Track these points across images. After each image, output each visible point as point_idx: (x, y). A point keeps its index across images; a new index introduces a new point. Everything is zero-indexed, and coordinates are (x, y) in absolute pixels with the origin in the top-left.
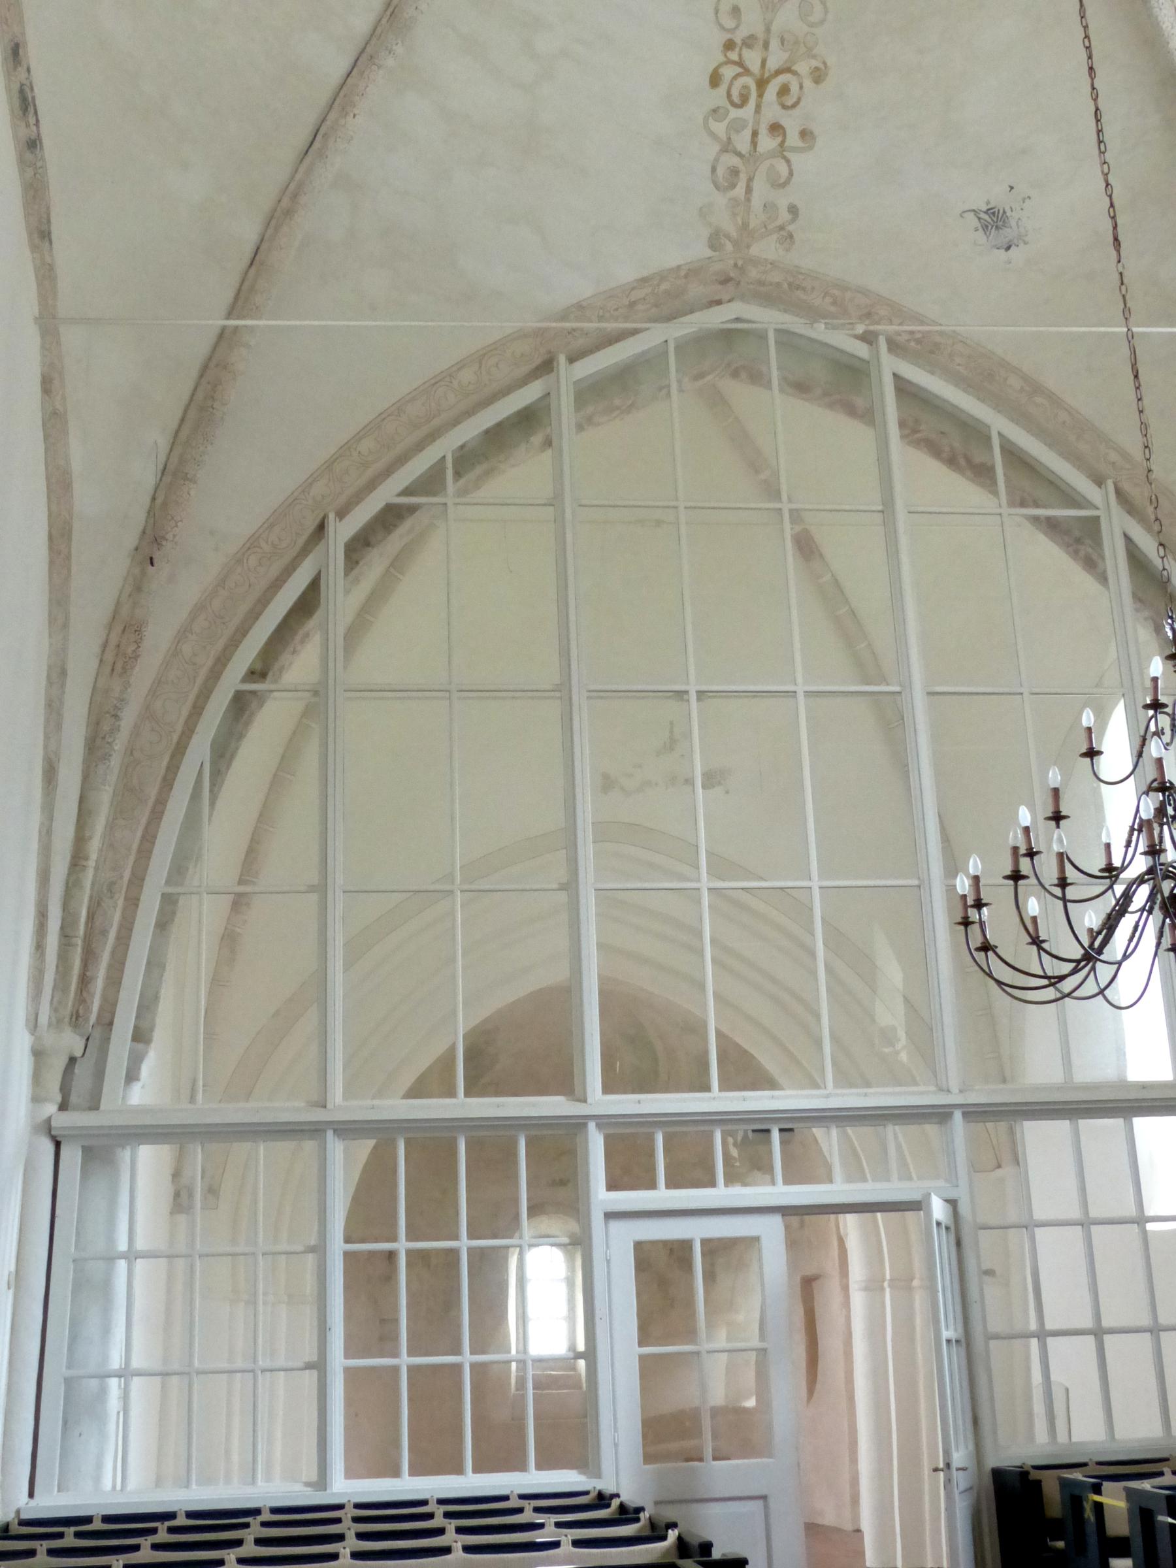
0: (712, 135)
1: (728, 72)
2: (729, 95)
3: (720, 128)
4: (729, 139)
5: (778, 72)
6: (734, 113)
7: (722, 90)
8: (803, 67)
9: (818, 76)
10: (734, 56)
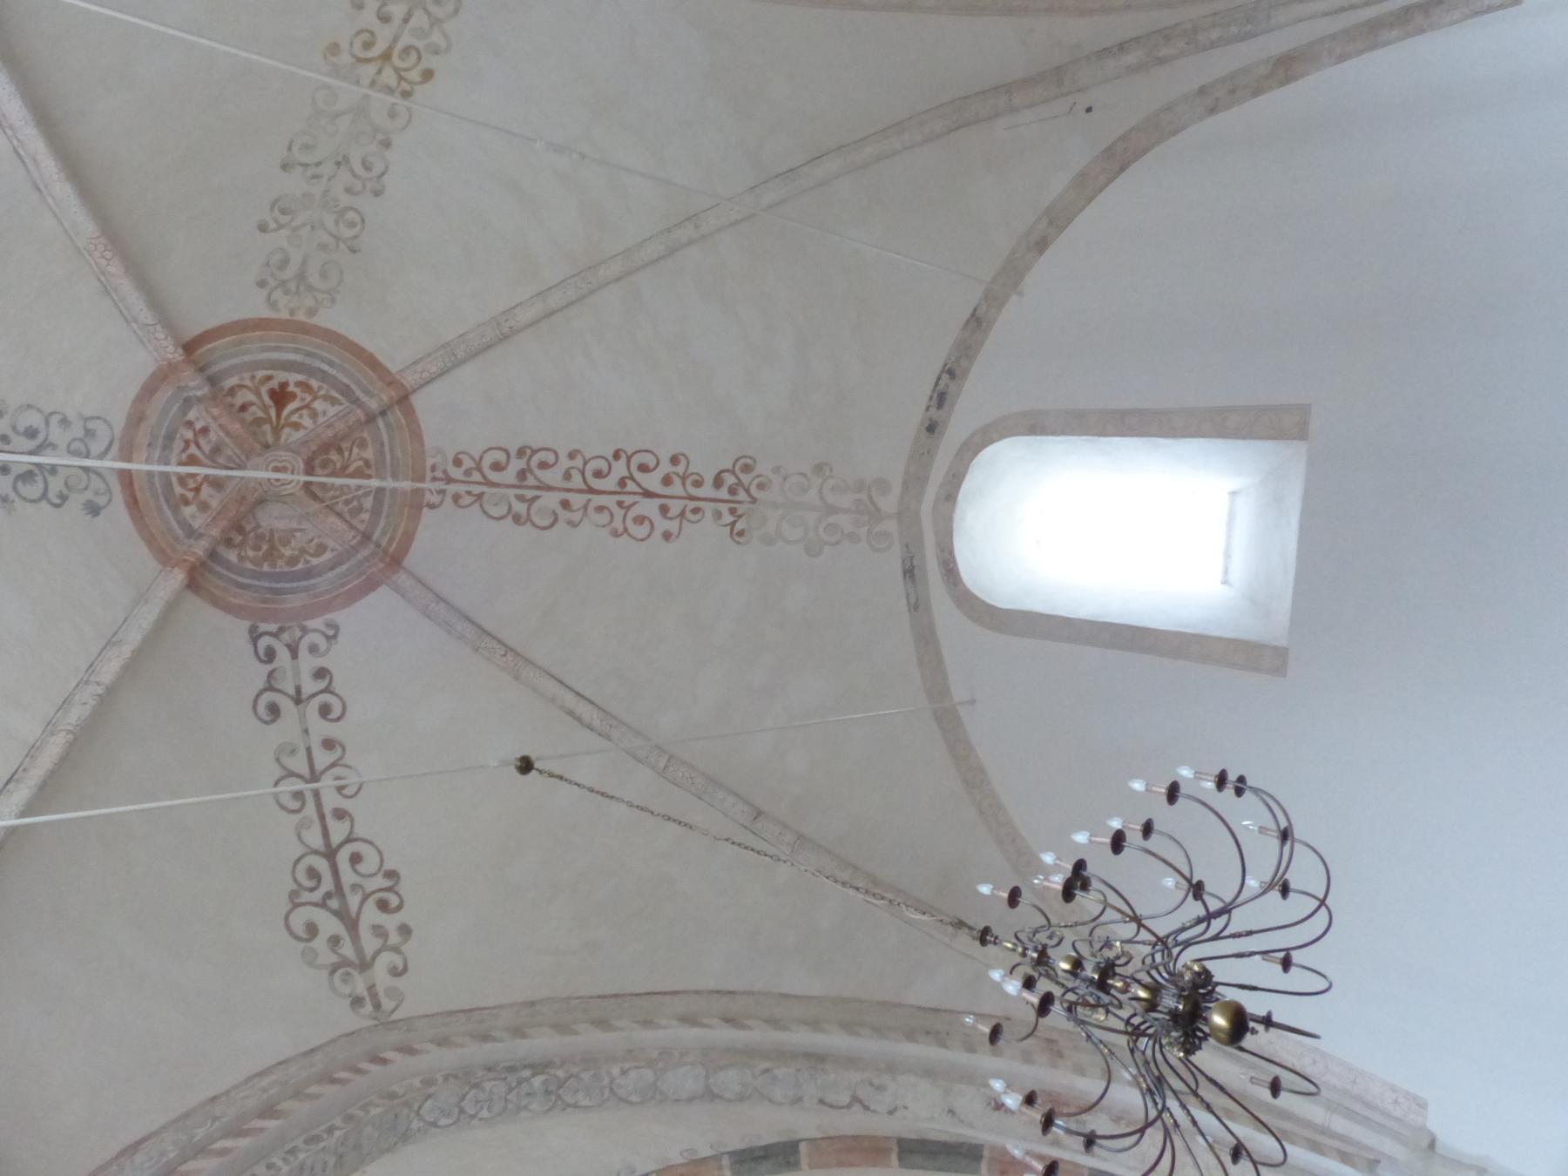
0: (445, 36)
1: (414, 75)
2: (420, 58)
3: (436, 38)
4: (432, 26)
5: (368, 61)
6: (420, 44)
7: (424, 65)
8: (345, 58)
9: (334, 48)
10: (405, 86)
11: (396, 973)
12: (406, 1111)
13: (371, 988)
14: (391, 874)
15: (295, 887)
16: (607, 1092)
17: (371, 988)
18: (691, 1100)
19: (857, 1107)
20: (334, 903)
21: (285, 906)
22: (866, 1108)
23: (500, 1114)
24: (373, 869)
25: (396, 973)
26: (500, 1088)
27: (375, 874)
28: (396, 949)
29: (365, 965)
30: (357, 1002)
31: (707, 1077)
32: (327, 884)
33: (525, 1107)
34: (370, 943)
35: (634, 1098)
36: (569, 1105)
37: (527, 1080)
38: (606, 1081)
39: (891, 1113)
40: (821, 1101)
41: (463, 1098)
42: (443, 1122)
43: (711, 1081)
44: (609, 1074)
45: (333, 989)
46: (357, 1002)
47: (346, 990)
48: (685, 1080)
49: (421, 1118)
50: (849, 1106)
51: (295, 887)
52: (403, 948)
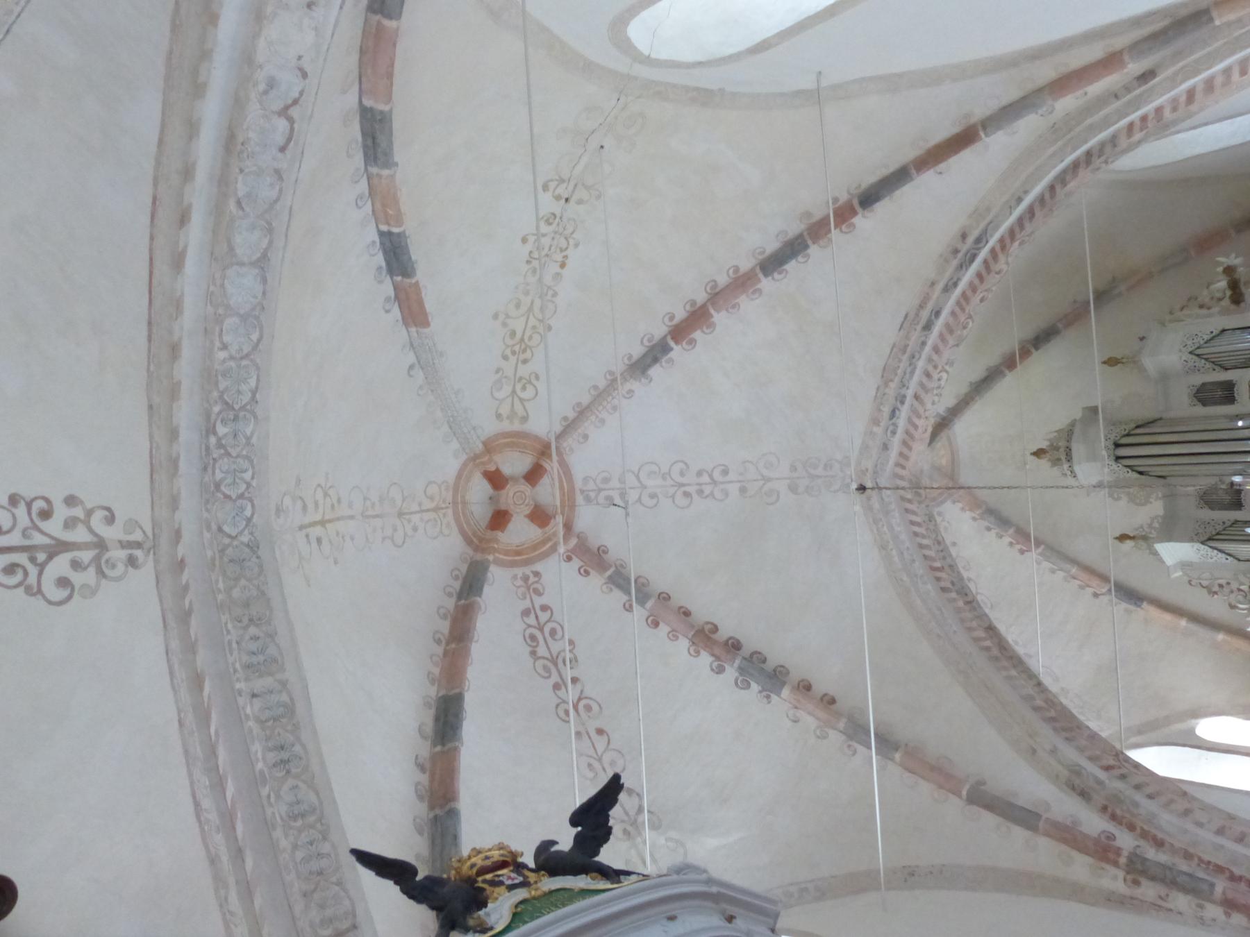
11: (111, 519)
12: (229, 551)
13: (124, 545)
14: (14, 500)
15: (22, 589)
16: (244, 363)
17: (124, 545)
18: (264, 281)
19: (294, 112)
20: (41, 557)
21: (38, 602)
22: (295, 102)
23: (251, 462)
24: (9, 515)
25: (111, 519)
26: (224, 464)
27: (14, 516)
28: (89, 513)
29: (101, 545)
30: (132, 562)
31: (242, 264)
32: (22, 558)
33: (248, 439)
34: (80, 535)
35: (255, 337)
36: (253, 398)
37: (219, 440)
38: (232, 364)
39: (305, 75)
40: (283, 149)
41: (227, 497)
42: (248, 513)
43: (246, 260)
44: (224, 361)
45: (118, 579)
46: (132, 562)
47: (121, 568)
48: (242, 288)
49: (241, 533)
50: (291, 120)
51: (22, 589)
52: (89, 506)
